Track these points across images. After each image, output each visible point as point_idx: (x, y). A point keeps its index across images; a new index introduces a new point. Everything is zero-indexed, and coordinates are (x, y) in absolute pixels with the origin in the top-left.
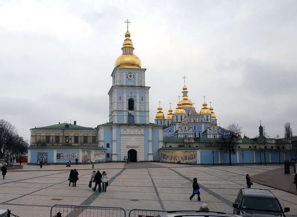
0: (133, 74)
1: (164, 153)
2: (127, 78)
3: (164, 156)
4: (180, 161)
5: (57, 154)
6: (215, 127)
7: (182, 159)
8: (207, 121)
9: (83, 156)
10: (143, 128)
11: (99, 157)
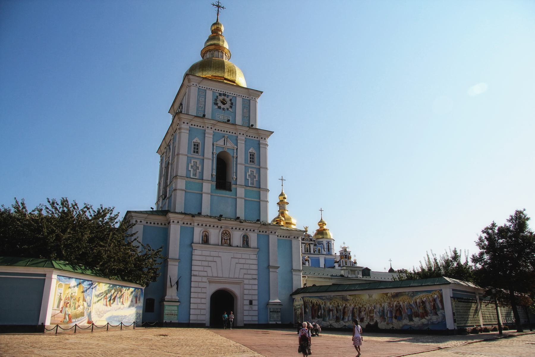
1: (315, 301)
2: (216, 104)
4: (376, 323)
6: (348, 261)
7: (383, 315)
8: (329, 251)
9: (60, 299)
10: (256, 231)
11: (122, 306)
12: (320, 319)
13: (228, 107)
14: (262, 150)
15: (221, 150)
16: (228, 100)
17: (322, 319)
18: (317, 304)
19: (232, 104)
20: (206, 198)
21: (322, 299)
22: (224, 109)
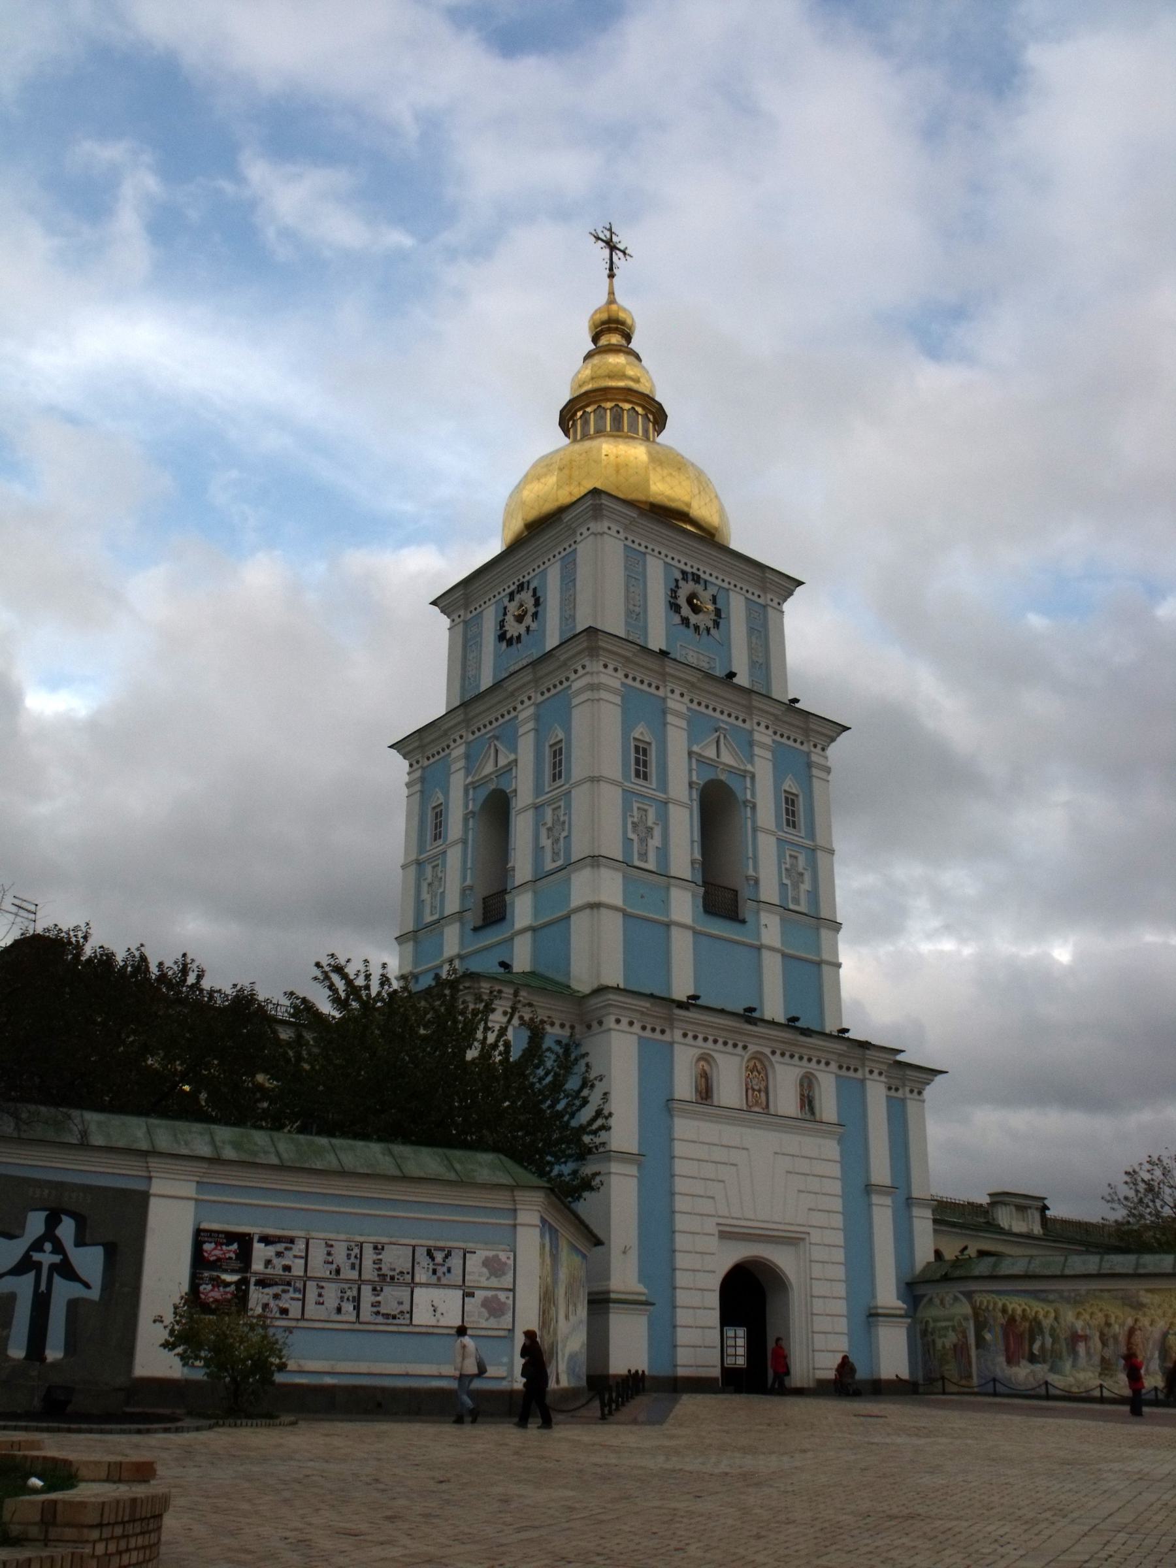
0: (712, 590)
1: (1016, 1305)
3: (1021, 1338)
5: (200, 1237)
12: (1038, 1367)
13: (710, 624)
14: (816, 783)
15: (710, 775)
16: (705, 596)
17: (1046, 1367)
18: (1024, 1316)
19: (718, 612)
20: (682, 946)
21: (1045, 1300)
22: (697, 628)
